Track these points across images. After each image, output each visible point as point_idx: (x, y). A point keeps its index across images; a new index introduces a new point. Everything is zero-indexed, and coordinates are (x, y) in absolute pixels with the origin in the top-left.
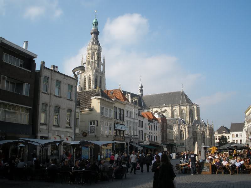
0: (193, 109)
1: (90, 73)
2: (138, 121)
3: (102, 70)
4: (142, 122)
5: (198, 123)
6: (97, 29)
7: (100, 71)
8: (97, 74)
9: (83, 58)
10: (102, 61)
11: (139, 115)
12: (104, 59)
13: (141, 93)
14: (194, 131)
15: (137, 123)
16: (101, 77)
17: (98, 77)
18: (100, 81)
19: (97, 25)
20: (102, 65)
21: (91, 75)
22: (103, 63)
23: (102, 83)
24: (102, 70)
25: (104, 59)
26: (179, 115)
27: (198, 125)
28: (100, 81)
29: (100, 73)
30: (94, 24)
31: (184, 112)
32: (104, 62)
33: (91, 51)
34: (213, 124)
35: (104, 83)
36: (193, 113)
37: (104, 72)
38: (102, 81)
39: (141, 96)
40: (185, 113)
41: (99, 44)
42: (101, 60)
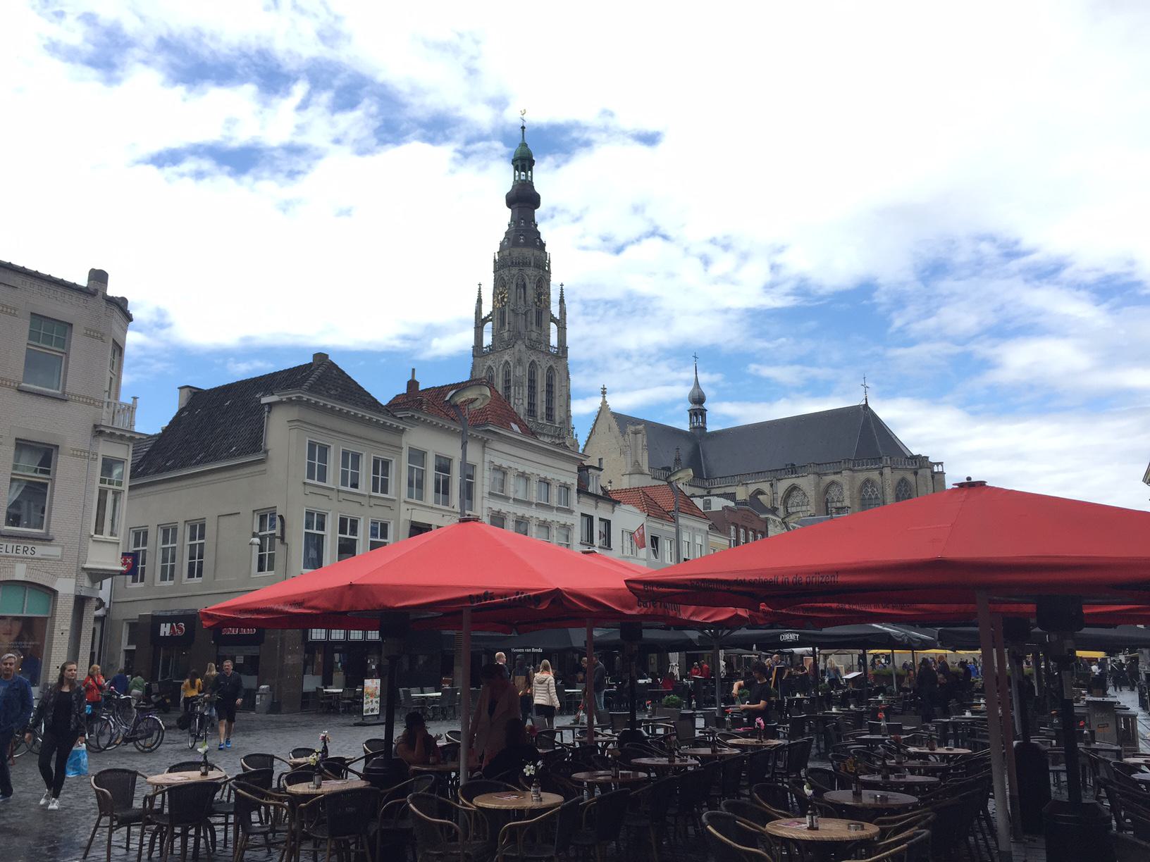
0: (910, 477)
1: (506, 357)
2: (576, 522)
3: (554, 341)
4: (608, 523)
6: (531, 184)
7: (548, 345)
8: (533, 358)
9: (479, 301)
10: (555, 310)
11: (583, 491)
12: (562, 301)
15: (567, 528)
17: (540, 371)
19: (531, 169)
20: (553, 327)
21: (512, 364)
22: (557, 315)
23: (557, 393)
24: (554, 341)
25: (562, 301)
29: (548, 353)
30: (519, 163)
31: (873, 491)
32: (563, 312)
33: (507, 272)
35: (564, 392)
38: (557, 384)
41: (541, 241)
42: (548, 307)
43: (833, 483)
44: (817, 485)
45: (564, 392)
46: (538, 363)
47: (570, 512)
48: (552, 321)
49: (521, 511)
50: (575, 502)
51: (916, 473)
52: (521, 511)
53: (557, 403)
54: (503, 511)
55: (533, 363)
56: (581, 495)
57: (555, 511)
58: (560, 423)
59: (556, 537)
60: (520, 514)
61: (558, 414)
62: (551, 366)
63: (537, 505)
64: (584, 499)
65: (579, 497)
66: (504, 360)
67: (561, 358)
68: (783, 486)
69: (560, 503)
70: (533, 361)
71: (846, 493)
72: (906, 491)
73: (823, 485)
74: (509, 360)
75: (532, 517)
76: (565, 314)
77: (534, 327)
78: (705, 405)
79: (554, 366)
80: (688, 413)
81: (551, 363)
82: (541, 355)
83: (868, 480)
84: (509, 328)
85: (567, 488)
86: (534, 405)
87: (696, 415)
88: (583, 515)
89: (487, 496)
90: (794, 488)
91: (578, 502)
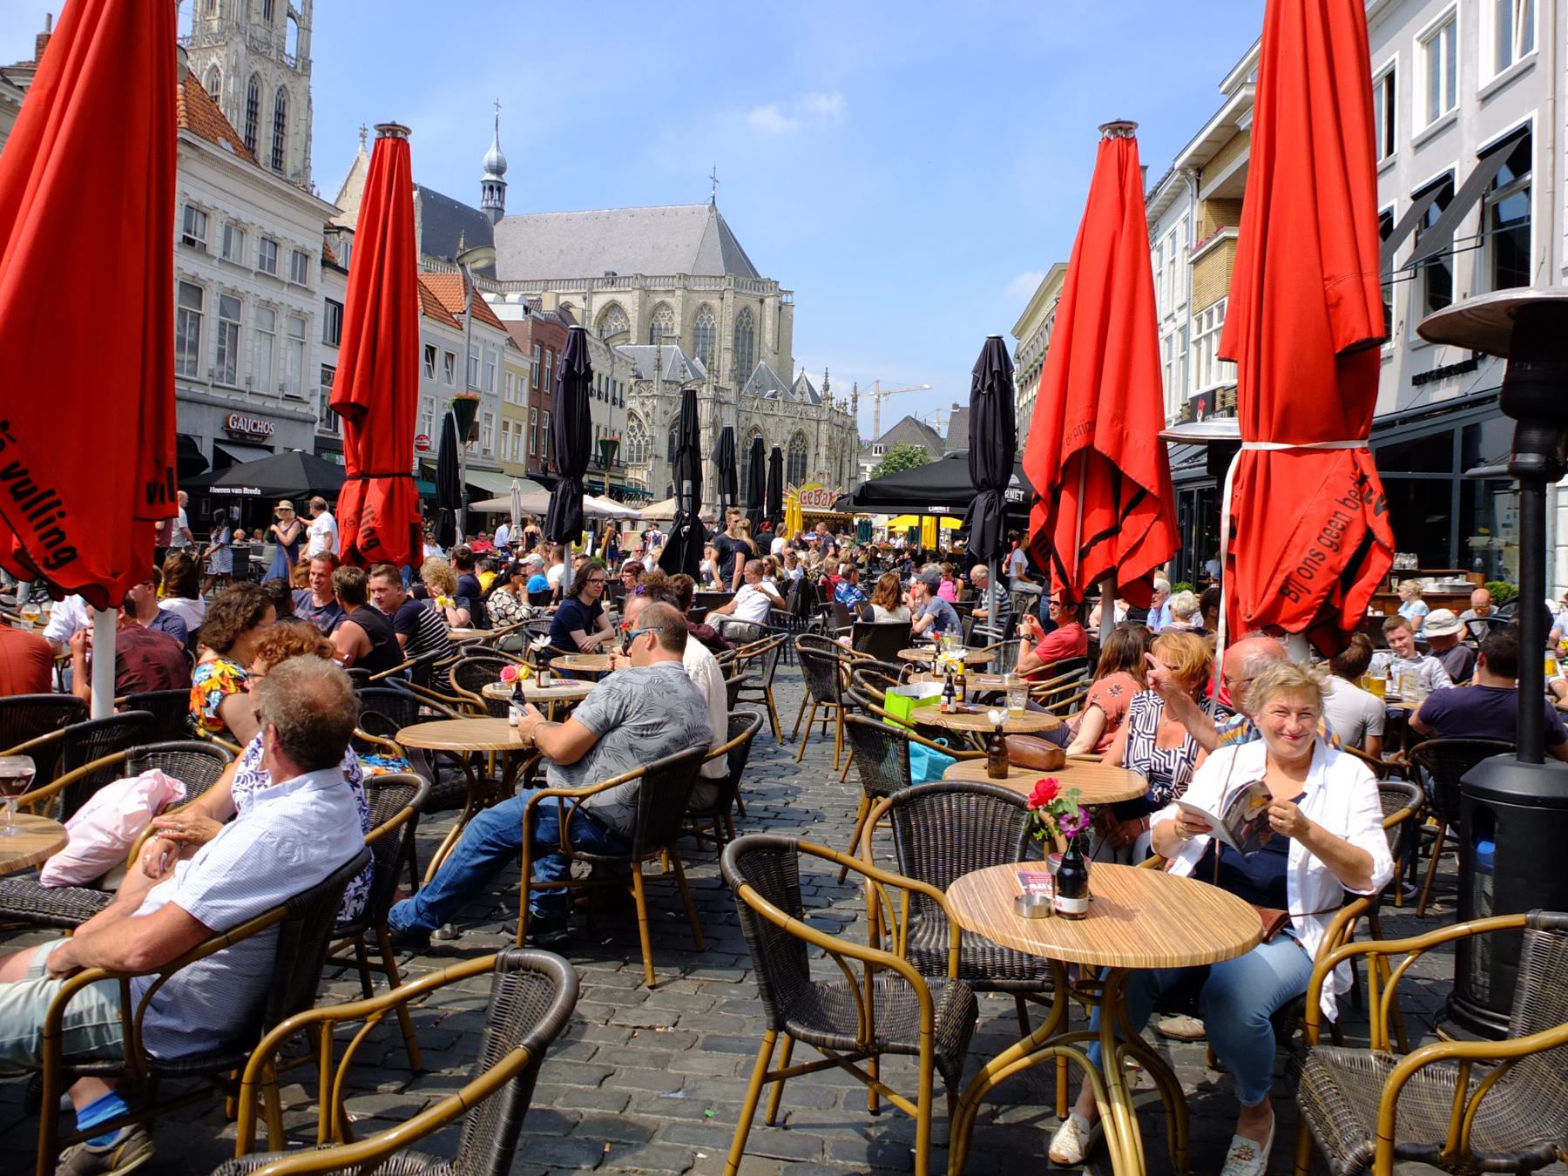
0: (755, 307)
1: (214, 60)
5: (775, 385)
7: (281, 51)
8: (258, 67)
13: (491, 204)
14: (752, 424)
15: (301, 318)
16: (282, 90)
18: (280, 116)
24: (291, 48)
26: (677, 332)
27: (774, 396)
28: (280, 116)
34: (855, 400)
36: (756, 331)
37: (303, 66)
38: (290, 112)
39: (491, 215)
40: (713, 329)
43: (663, 304)
44: (642, 304)
45: (302, 128)
46: (263, 77)
47: (309, 292)
48: (290, 15)
49: (231, 280)
50: (318, 279)
51: (762, 301)
52: (231, 280)
53: (290, 145)
54: (201, 276)
55: (254, 77)
56: (327, 270)
57: (285, 288)
58: (293, 175)
59: (284, 326)
60: (229, 285)
61: (291, 161)
62: (284, 86)
63: (257, 274)
64: (332, 275)
65: (324, 273)
66: (210, 64)
67: (300, 75)
68: (599, 302)
69: (294, 277)
70: (257, 73)
71: (678, 319)
72: (748, 323)
73: (649, 306)
74: (218, 64)
75: (248, 292)
76: (311, 7)
77: (257, 19)
78: (506, 177)
79: (289, 87)
80: (481, 186)
81: (285, 80)
82: (270, 65)
83: (705, 305)
84: (221, 13)
85: (302, 257)
86: (254, 141)
87: (491, 188)
88: (328, 300)
90: (613, 307)
91: (322, 280)
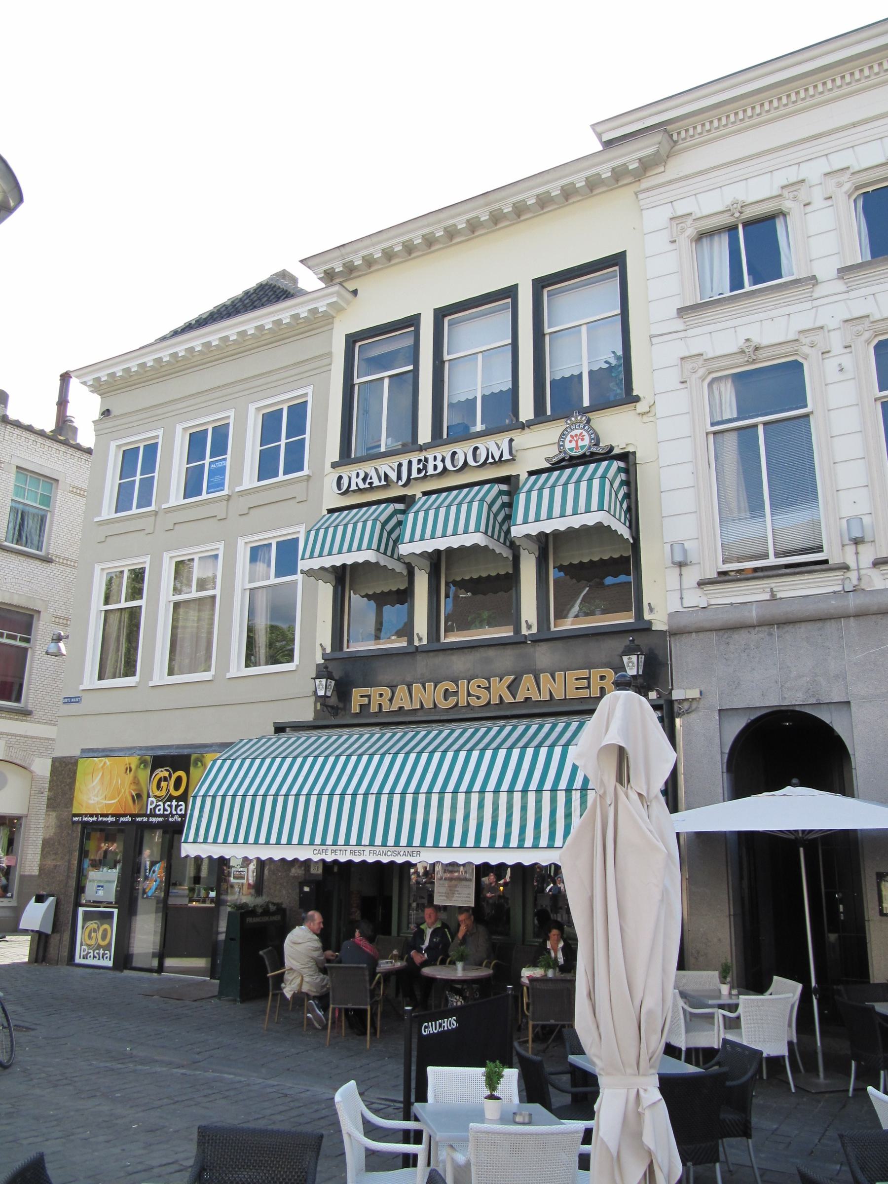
89: (679, 324)
